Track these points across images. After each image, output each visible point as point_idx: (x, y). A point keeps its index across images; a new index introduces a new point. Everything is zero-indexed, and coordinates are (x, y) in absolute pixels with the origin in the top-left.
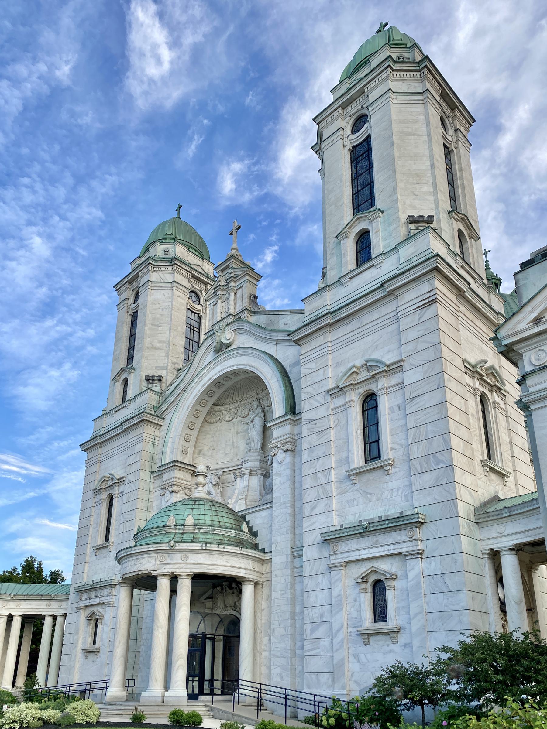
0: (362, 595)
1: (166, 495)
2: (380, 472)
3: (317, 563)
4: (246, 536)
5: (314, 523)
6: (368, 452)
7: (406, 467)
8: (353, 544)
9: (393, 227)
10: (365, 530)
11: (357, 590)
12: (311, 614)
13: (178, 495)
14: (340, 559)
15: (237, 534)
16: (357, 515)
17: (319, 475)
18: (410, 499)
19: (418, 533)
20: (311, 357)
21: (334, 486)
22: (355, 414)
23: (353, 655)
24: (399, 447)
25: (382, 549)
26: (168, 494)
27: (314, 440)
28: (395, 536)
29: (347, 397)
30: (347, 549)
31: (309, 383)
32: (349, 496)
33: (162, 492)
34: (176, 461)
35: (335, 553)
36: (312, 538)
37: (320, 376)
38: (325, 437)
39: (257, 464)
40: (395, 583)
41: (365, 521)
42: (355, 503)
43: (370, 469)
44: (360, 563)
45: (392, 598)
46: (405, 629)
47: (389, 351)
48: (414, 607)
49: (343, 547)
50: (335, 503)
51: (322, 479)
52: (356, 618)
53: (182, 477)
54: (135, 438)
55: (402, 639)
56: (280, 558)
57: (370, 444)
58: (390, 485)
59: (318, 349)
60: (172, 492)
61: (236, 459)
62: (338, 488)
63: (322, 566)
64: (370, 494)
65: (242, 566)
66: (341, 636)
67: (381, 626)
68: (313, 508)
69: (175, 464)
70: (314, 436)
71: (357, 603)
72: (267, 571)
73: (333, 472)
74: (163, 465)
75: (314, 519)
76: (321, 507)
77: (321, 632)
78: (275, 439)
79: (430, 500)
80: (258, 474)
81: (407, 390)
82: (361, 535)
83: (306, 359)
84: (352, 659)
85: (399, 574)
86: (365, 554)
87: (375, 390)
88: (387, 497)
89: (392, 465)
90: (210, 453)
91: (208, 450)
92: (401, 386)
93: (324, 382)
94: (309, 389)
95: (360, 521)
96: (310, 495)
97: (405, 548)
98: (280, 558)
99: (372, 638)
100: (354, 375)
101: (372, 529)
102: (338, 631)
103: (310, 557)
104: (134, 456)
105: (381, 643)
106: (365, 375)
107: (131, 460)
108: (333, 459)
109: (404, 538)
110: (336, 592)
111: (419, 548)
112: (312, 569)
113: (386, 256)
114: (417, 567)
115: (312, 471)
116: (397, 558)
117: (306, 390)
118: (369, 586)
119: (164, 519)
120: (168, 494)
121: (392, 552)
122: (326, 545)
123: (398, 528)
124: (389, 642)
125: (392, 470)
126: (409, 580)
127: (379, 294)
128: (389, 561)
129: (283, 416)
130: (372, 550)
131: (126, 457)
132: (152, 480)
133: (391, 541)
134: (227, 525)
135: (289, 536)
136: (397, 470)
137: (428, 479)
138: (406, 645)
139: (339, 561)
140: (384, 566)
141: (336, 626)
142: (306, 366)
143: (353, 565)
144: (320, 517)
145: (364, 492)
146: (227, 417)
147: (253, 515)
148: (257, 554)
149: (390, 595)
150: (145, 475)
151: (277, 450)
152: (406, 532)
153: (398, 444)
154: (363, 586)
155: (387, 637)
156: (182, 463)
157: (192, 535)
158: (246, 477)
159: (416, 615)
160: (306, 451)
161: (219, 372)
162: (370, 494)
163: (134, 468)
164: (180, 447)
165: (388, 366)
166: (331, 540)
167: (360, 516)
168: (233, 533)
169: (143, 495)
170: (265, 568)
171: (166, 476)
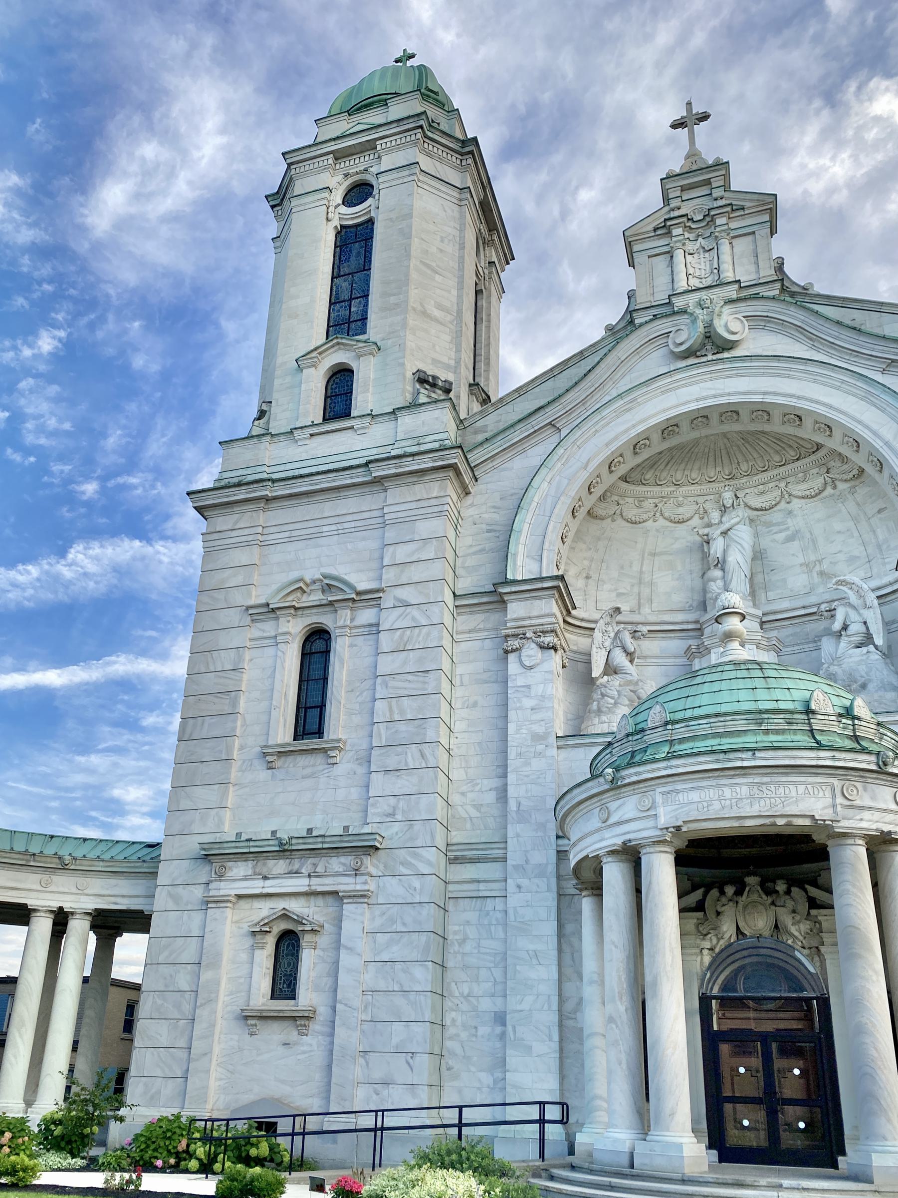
54: (414, 505)
91: (577, 576)
104: (412, 546)
131: (374, 545)
161: (664, 411)
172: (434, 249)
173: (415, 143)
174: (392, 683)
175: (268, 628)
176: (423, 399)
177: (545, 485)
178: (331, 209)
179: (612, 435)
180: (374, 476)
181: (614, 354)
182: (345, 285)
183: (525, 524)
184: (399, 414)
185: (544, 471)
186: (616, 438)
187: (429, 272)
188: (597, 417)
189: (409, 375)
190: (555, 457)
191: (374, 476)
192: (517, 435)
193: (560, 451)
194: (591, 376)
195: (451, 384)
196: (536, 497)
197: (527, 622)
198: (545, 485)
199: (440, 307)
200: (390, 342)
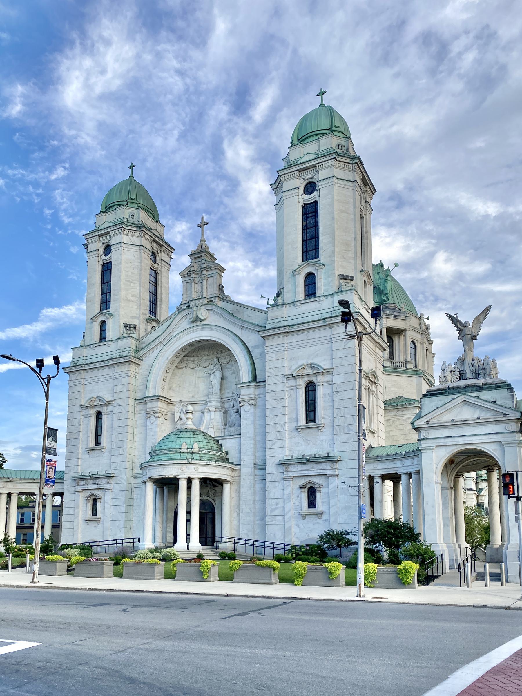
0: (303, 494)
1: (151, 418)
3: (275, 475)
4: (224, 455)
5: (273, 453)
6: (308, 416)
7: (332, 429)
8: (299, 467)
9: (331, 279)
10: (306, 461)
11: (299, 491)
12: (271, 503)
13: (161, 419)
14: (290, 475)
15: (221, 454)
16: (301, 452)
17: (278, 426)
18: (332, 446)
19: (337, 465)
20: (273, 349)
21: (287, 433)
22: (302, 392)
24: (327, 417)
25: (315, 471)
26: (152, 418)
27: (274, 403)
29: (298, 382)
30: (295, 469)
31: (271, 367)
32: (296, 440)
33: (149, 416)
34: (159, 396)
35: (287, 471)
36: (272, 460)
37: (279, 364)
38: (282, 403)
39: (218, 404)
40: (321, 489)
41: (308, 456)
42: (300, 444)
45: (319, 497)
46: (325, 512)
47: (325, 360)
48: (332, 502)
49: (292, 468)
50: (287, 443)
51: (279, 428)
53: (162, 407)
55: (324, 517)
56: (247, 470)
57: (309, 412)
58: (321, 438)
59: (278, 346)
60: (156, 417)
61: (197, 396)
62: (289, 435)
63: (279, 477)
65: (225, 473)
66: (290, 514)
67: (312, 510)
68: (273, 445)
69: (158, 397)
70: (274, 401)
71: (299, 498)
72: (236, 475)
73: (287, 425)
74: (147, 397)
75: (273, 450)
76: (278, 444)
77: (277, 512)
78: (242, 396)
79: (343, 449)
80: (220, 411)
81: (335, 386)
82: (304, 463)
83: (270, 350)
85: (324, 485)
86: (306, 473)
87: (315, 381)
88: (317, 444)
89: (323, 427)
90: (177, 389)
92: (331, 383)
93: (282, 368)
94: (272, 371)
95: (303, 456)
96: (270, 437)
97: (329, 472)
98: (247, 470)
99: (307, 516)
100: (303, 369)
102: (288, 512)
103: (270, 472)
105: (312, 519)
106: (309, 371)
107: (119, 388)
108: (287, 417)
109: (328, 467)
110: (287, 492)
111: (336, 473)
112: (272, 478)
113: (326, 297)
114: (334, 483)
115: (272, 422)
116: (323, 476)
117: (269, 370)
118: (306, 490)
119: (177, 443)
120: (152, 418)
121: (321, 474)
122: (281, 466)
123: (326, 462)
124: (317, 518)
125: (323, 430)
126: (330, 488)
127: (321, 323)
128: (318, 478)
129: (246, 383)
130: (310, 472)
132: (136, 405)
133: (321, 468)
134: (215, 448)
135: (253, 457)
137: (344, 438)
138: (326, 520)
139: (289, 475)
141: (286, 510)
142: (269, 355)
143: (298, 478)
144: (277, 450)
145: (305, 439)
146: (191, 365)
147: (224, 440)
148: (230, 465)
149: (319, 496)
150: (132, 402)
151: (244, 403)
152: (329, 464)
153: (327, 416)
154: (303, 490)
155: (316, 516)
156: (163, 397)
157: (198, 455)
158: (212, 413)
159: (333, 506)
160: (269, 410)
163: (122, 395)
164: (161, 385)
165: (325, 370)
166: (284, 464)
167: (302, 452)
168: (219, 453)
169: (131, 416)
170: (236, 474)
171: (150, 405)
172: (130, 274)
173: (121, 233)
174: (116, 430)
175: (85, 412)
176: (125, 335)
177: (157, 364)
178: (99, 257)
179: (174, 349)
180: (112, 363)
181: (175, 320)
182: (105, 287)
183: (152, 378)
184: (118, 340)
185: (156, 360)
186: (174, 350)
187: (128, 283)
188: (170, 343)
189: (122, 325)
190: (159, 356)
191: (112, 363)
192: (151, 346)
193: (161, 354)
194: (169, 328)
195: (136, 325)
196: (155, 369)
197: (152, 409)
198: (157, 364)
199: (133, 296)
200: (116, 313)
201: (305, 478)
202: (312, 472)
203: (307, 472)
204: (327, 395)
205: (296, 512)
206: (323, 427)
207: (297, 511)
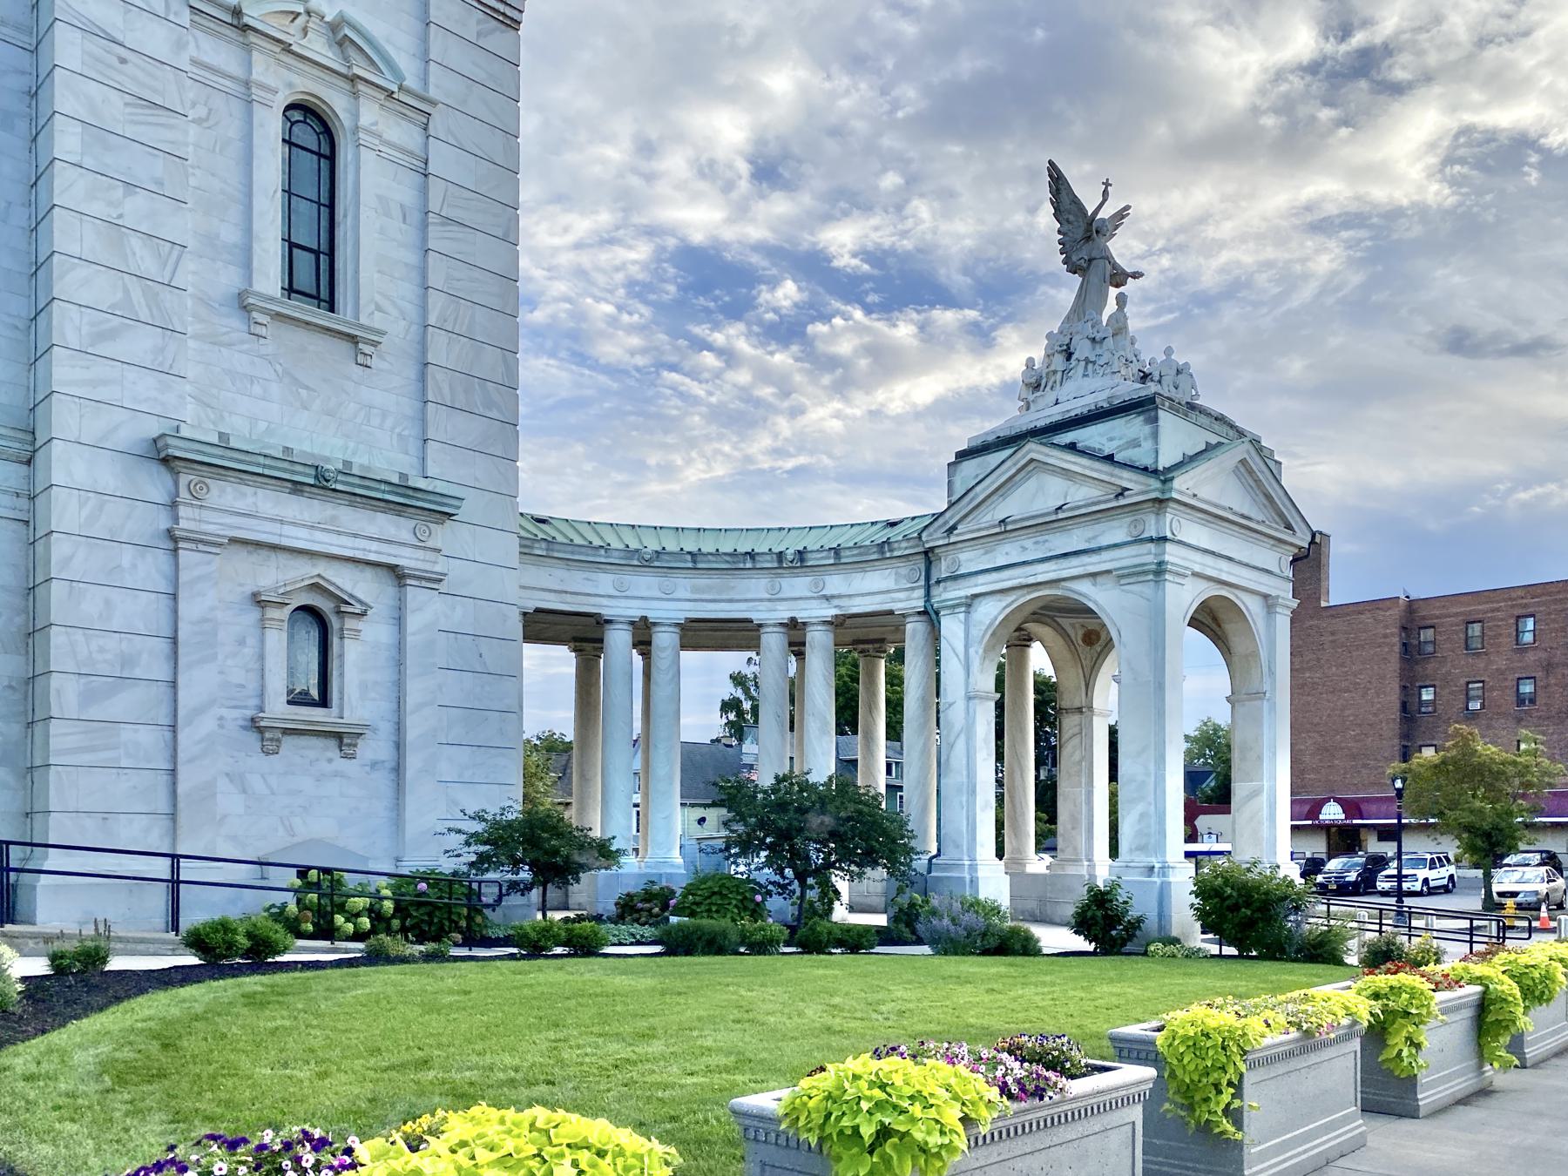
2: (345, 346)
23: (227, 775)
25: (344, 540)
28: (384, 524)
42: (257, 390)
43: (316, 325)
44: (264, 553)
52: (243, 686)
64: (307, 388)
66: (207, 725)
84: (223, 784)
89: (375, 344)
101: (339, 487)
130: (319, 535)
136: (384, 365)
140: (344, 580)
143: (242, 553)
162: (307, 388)
201: (283, 558)
202: (334, 538)
203: (303, 533)
204: (397, 213)
205: (231, 714)
206: (375, 344)
207: (237, 713)
